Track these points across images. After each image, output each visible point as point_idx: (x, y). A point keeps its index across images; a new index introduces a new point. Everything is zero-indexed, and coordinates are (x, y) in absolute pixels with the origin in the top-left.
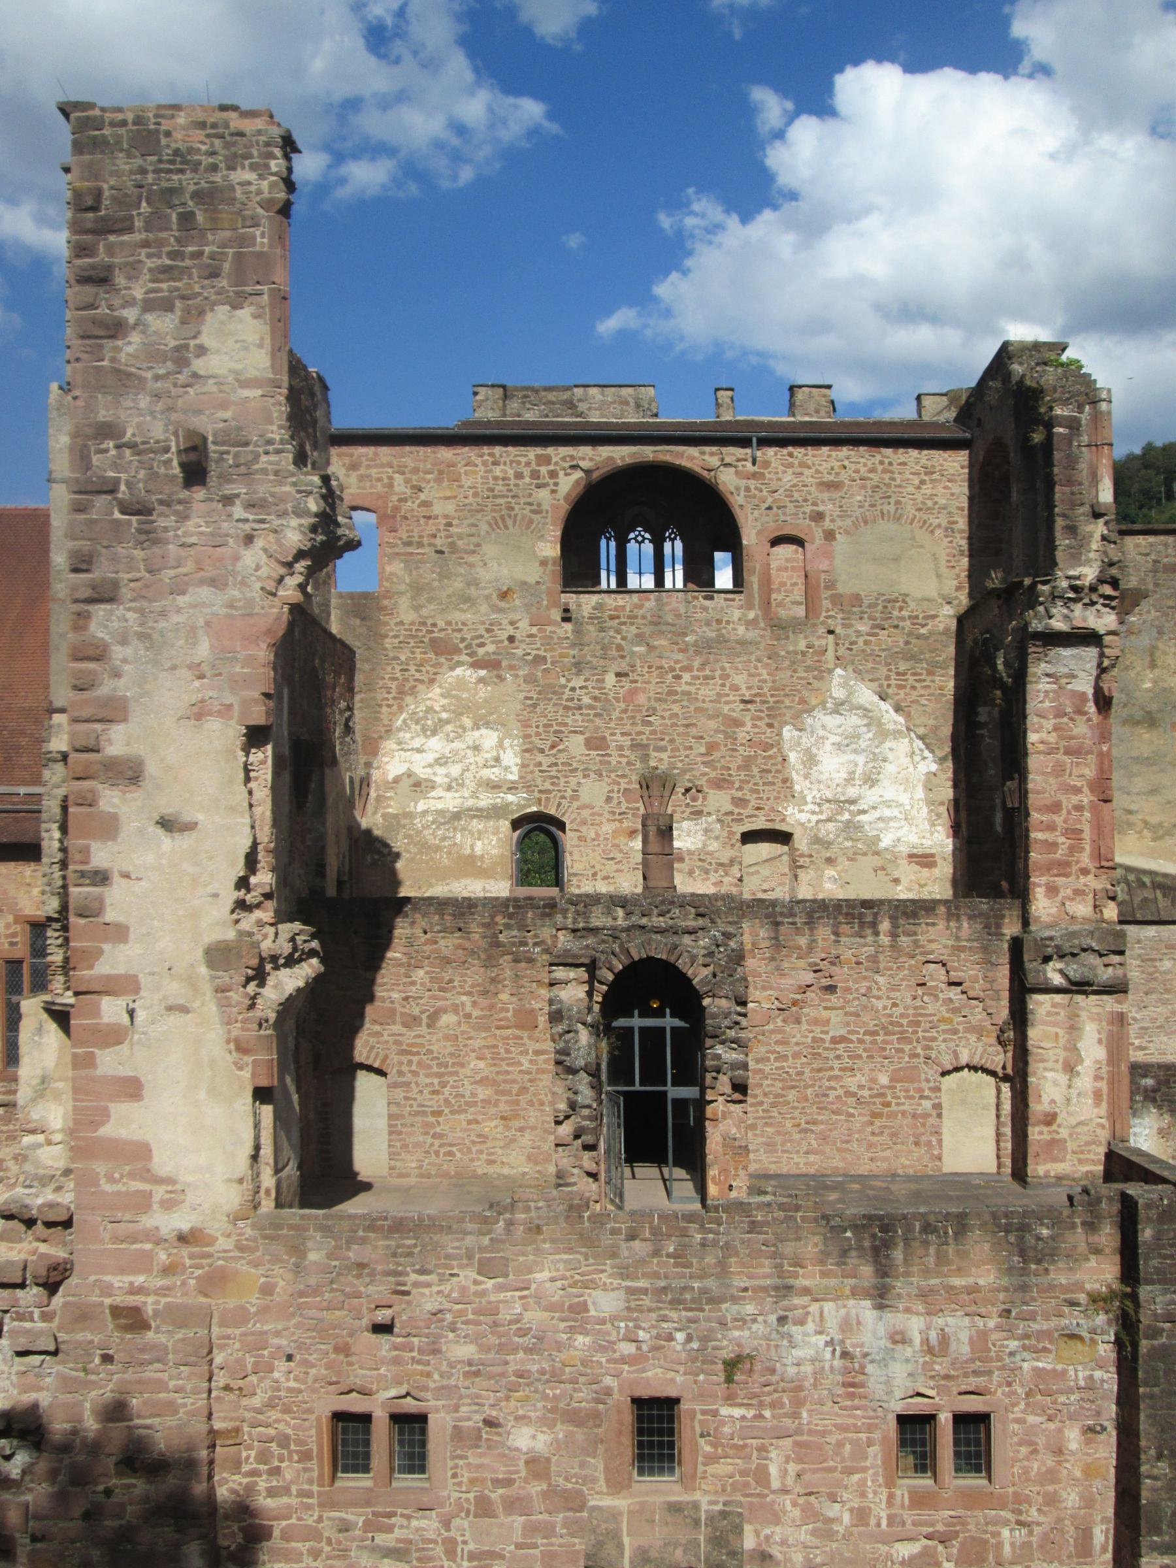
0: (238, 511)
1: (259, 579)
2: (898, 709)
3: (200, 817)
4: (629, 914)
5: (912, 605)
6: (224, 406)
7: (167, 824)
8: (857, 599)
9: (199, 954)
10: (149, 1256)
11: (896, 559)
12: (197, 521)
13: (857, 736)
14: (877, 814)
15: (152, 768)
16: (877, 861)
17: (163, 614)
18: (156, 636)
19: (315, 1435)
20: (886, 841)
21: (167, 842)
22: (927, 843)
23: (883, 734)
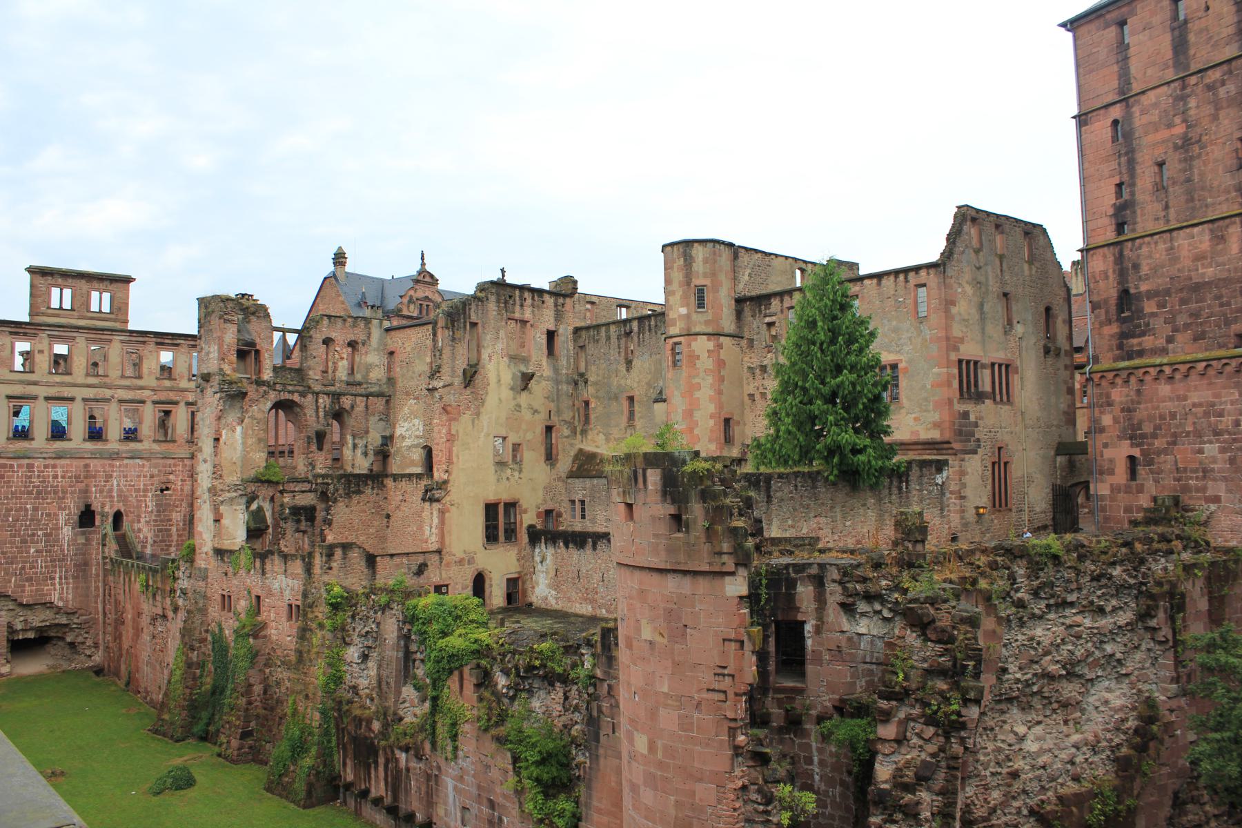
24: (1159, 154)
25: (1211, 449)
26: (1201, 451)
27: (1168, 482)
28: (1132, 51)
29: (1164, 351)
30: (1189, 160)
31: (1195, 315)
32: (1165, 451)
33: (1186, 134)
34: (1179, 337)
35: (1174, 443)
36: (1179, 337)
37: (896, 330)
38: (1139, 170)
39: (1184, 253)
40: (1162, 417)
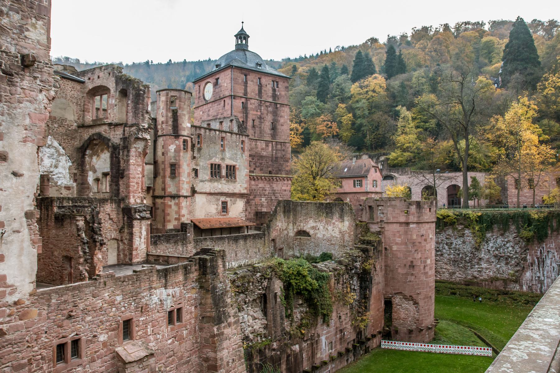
0: (38, 82)
1: (43, 103)
2: (63, 148)
3: (24, 172)
4: (73, 202)
5: (68, 122)
6: (33, 49)
7: (15, 174)
8: (55, 118)
9: (23, 214)
10: (4, 311)
11: (65, 109)
12: (25, 82)
13: (53, 155)
14: (57, 176)
15: (10, 156)
16: (57, 188)
17: (15, 108)
18: (13, 115)
19: (49, 353)
20: (59, 183)
21: (15, 179)
22: (69, 184)
23: (60, 155)
24: (254, 117)
25: (263, 199)
26: (261, 200)
27: (253, 208)
28: (248, 85)
29: (253, 172)
30: (261, 122)
31: (261, 164)
32: (253, 200)
33: (260, 116)
34: (257, 169)
35: (255, 197)
36: (257, 169)
37: (236, 154)
38: (248, 120)
39: (259, 147)
40: (252, 190)
